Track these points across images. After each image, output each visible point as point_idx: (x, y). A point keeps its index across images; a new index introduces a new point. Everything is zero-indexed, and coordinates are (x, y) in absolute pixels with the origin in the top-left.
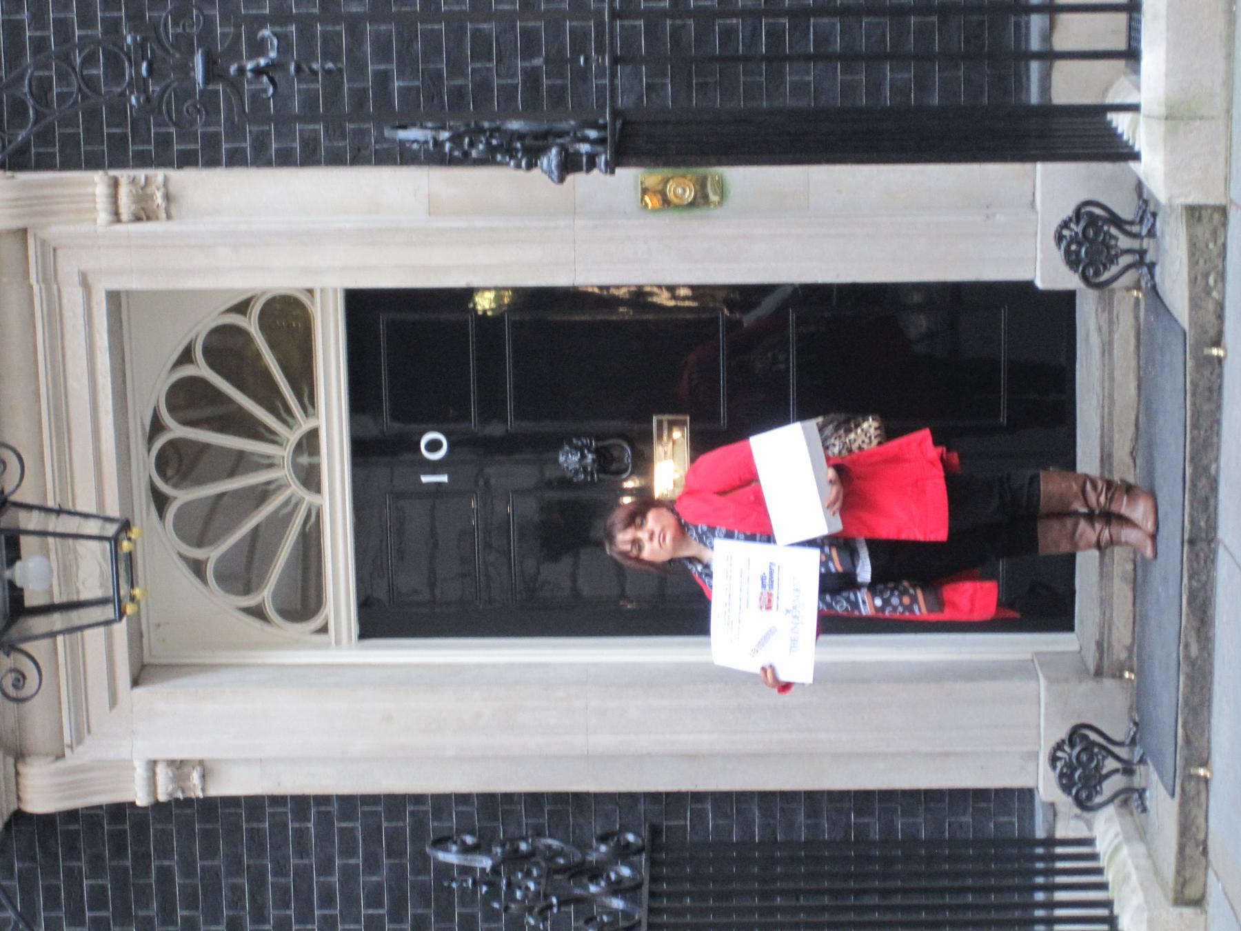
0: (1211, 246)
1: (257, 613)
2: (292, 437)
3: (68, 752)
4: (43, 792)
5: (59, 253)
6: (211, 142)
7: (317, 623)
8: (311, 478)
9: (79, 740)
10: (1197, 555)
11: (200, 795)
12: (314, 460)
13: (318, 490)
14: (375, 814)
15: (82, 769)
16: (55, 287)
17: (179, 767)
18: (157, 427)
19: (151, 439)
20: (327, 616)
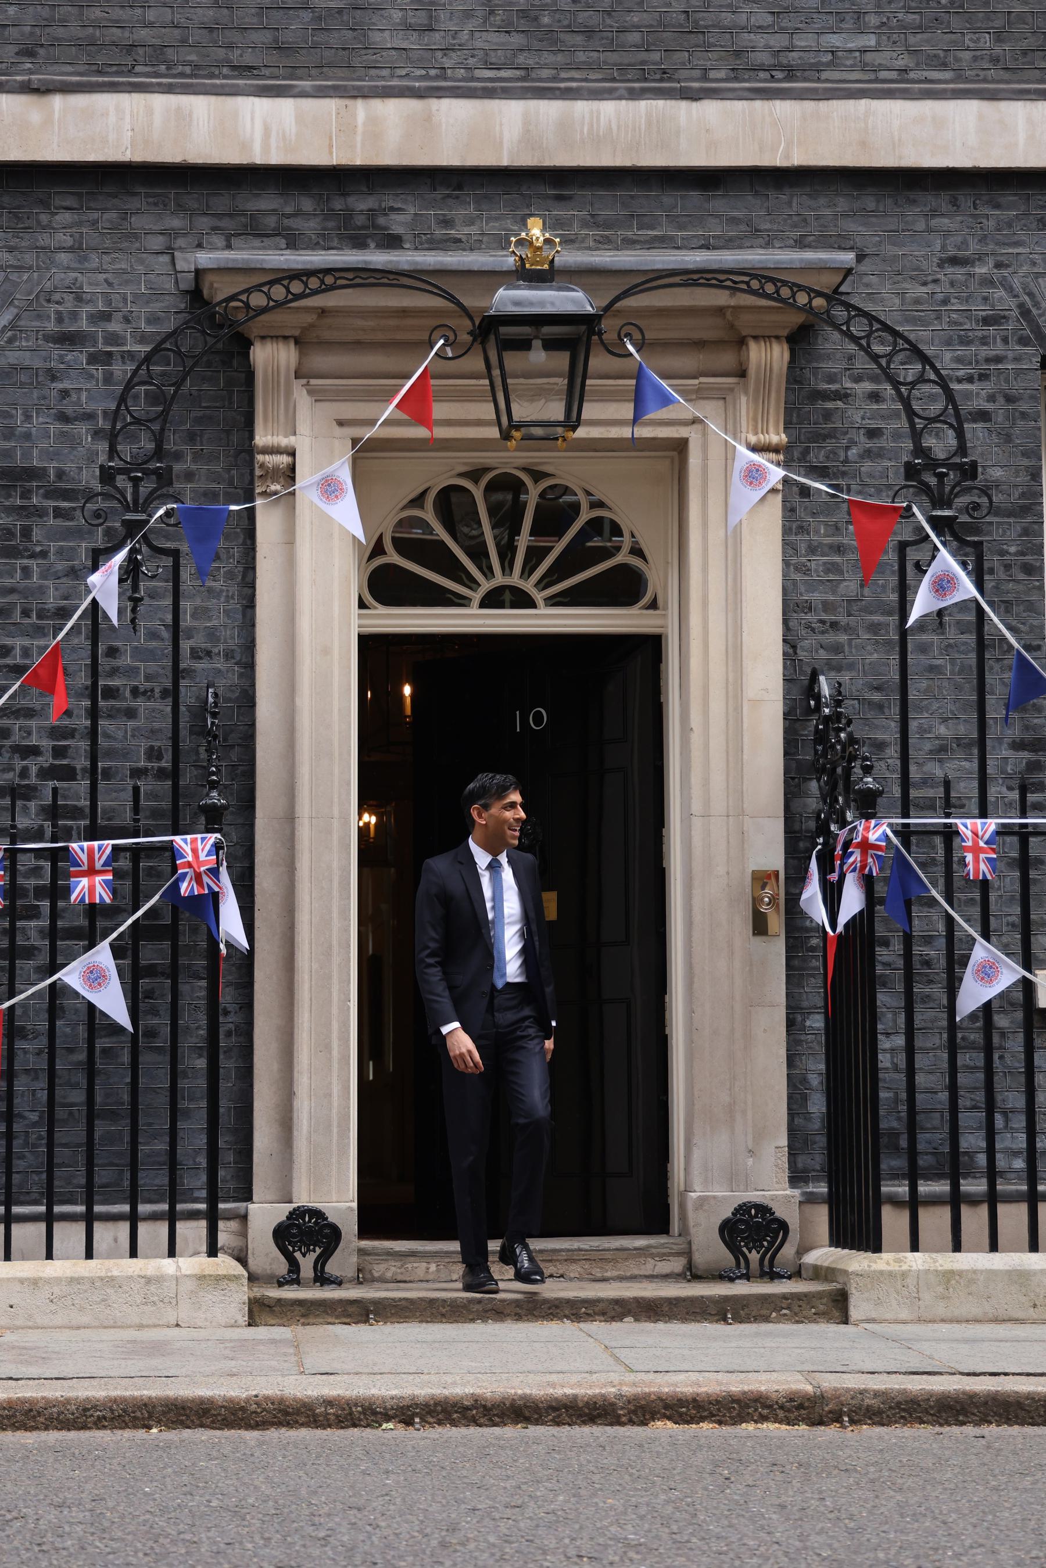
0: (813, 1310)
1: (378, 549)
2: (528, 586)
3: (304, 381)
4: (270, 358)
5: (721, 403)
6: (802, 529)
7: (369, 599)
8: (493, 600)
9: (310, 393)
10: (557, 1307)
11: (258, 490)
12: (507, 604)
13: (482, 605)
14: (233, 638)
15: (289, 393)
16: (694, 397)
17: (290, 474)
18: (538, 476)
19: (525, 469)
20: (376, 608)
